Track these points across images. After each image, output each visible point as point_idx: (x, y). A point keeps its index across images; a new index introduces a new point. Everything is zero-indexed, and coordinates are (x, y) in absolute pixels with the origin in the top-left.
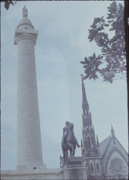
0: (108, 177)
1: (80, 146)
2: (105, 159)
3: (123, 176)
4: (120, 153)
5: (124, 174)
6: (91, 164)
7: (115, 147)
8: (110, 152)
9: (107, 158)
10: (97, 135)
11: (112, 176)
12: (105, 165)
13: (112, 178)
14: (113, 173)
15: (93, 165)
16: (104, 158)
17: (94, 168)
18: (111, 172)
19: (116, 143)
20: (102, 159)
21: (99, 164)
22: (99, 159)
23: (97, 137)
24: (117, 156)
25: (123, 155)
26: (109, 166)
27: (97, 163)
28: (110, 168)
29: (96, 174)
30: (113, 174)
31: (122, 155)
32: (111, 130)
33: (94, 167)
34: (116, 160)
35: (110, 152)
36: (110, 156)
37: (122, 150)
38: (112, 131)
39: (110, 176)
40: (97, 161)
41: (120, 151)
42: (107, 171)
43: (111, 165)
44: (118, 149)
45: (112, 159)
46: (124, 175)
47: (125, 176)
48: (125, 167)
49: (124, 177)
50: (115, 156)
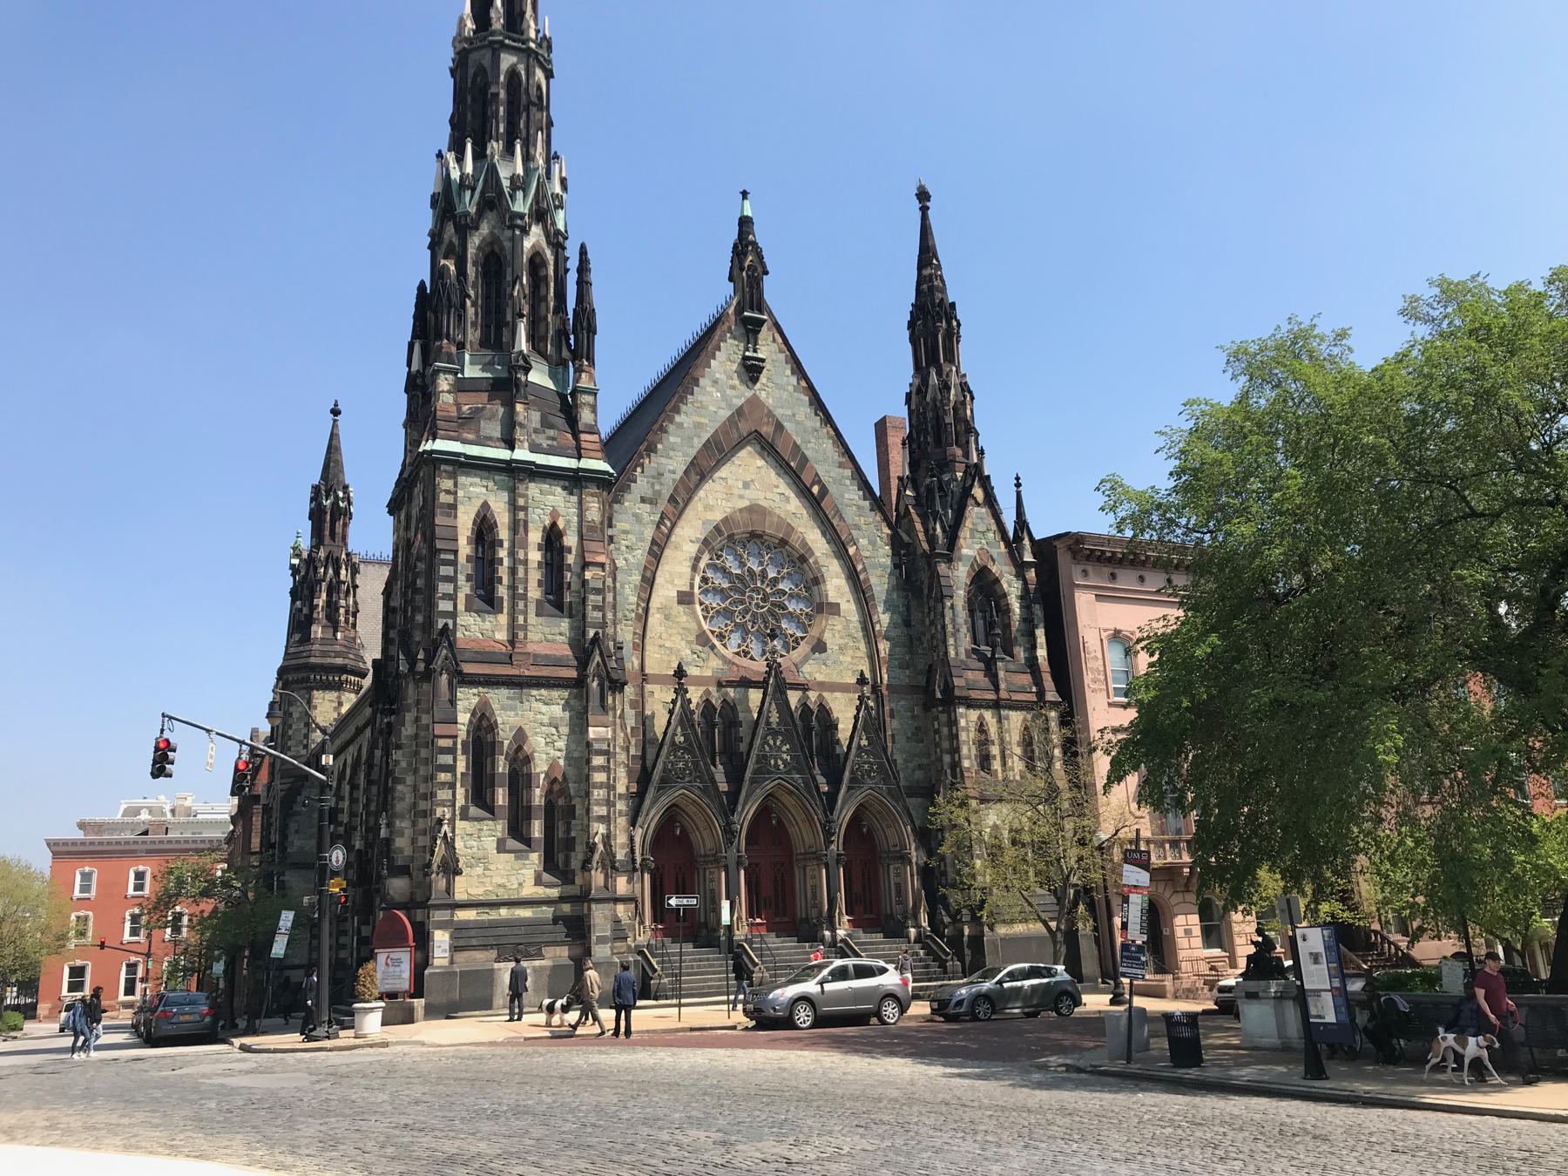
0: (660, 679)
2: (643, 500)
3: (803, 688)
4: (792, 468)
5: (813, 671)
6: (484, 529)
7: (754, 402)
10: (583, 251)
11: (699, 681)
12: (640, 555)
13: (695, 695)
14: (713, 647)
15: (504, 534)
16: (641, 485)
18: (692, 638)
19: (767, 365)
20: (612, 487)
21: (571, 540)
22: (575, 481)
23: (583, 268)
24: (757, 495)
25: (824, 491)
26: (676, 572)
27: (555, 514)
28: (685, 598)
29: (525, 628)
30: (715, 663)
31: (815, 489)
32: (735, 246)
33: (503, 553)
34: (745, 535)
35: (698, 444)
39: (680, 673)
42: (654, 619)
43: (694, 568)
44: (779, 427)
45: (718, 516)
46: (820, 678)
48: (835, 609)
49: (813, 695)
50: (746, 485)
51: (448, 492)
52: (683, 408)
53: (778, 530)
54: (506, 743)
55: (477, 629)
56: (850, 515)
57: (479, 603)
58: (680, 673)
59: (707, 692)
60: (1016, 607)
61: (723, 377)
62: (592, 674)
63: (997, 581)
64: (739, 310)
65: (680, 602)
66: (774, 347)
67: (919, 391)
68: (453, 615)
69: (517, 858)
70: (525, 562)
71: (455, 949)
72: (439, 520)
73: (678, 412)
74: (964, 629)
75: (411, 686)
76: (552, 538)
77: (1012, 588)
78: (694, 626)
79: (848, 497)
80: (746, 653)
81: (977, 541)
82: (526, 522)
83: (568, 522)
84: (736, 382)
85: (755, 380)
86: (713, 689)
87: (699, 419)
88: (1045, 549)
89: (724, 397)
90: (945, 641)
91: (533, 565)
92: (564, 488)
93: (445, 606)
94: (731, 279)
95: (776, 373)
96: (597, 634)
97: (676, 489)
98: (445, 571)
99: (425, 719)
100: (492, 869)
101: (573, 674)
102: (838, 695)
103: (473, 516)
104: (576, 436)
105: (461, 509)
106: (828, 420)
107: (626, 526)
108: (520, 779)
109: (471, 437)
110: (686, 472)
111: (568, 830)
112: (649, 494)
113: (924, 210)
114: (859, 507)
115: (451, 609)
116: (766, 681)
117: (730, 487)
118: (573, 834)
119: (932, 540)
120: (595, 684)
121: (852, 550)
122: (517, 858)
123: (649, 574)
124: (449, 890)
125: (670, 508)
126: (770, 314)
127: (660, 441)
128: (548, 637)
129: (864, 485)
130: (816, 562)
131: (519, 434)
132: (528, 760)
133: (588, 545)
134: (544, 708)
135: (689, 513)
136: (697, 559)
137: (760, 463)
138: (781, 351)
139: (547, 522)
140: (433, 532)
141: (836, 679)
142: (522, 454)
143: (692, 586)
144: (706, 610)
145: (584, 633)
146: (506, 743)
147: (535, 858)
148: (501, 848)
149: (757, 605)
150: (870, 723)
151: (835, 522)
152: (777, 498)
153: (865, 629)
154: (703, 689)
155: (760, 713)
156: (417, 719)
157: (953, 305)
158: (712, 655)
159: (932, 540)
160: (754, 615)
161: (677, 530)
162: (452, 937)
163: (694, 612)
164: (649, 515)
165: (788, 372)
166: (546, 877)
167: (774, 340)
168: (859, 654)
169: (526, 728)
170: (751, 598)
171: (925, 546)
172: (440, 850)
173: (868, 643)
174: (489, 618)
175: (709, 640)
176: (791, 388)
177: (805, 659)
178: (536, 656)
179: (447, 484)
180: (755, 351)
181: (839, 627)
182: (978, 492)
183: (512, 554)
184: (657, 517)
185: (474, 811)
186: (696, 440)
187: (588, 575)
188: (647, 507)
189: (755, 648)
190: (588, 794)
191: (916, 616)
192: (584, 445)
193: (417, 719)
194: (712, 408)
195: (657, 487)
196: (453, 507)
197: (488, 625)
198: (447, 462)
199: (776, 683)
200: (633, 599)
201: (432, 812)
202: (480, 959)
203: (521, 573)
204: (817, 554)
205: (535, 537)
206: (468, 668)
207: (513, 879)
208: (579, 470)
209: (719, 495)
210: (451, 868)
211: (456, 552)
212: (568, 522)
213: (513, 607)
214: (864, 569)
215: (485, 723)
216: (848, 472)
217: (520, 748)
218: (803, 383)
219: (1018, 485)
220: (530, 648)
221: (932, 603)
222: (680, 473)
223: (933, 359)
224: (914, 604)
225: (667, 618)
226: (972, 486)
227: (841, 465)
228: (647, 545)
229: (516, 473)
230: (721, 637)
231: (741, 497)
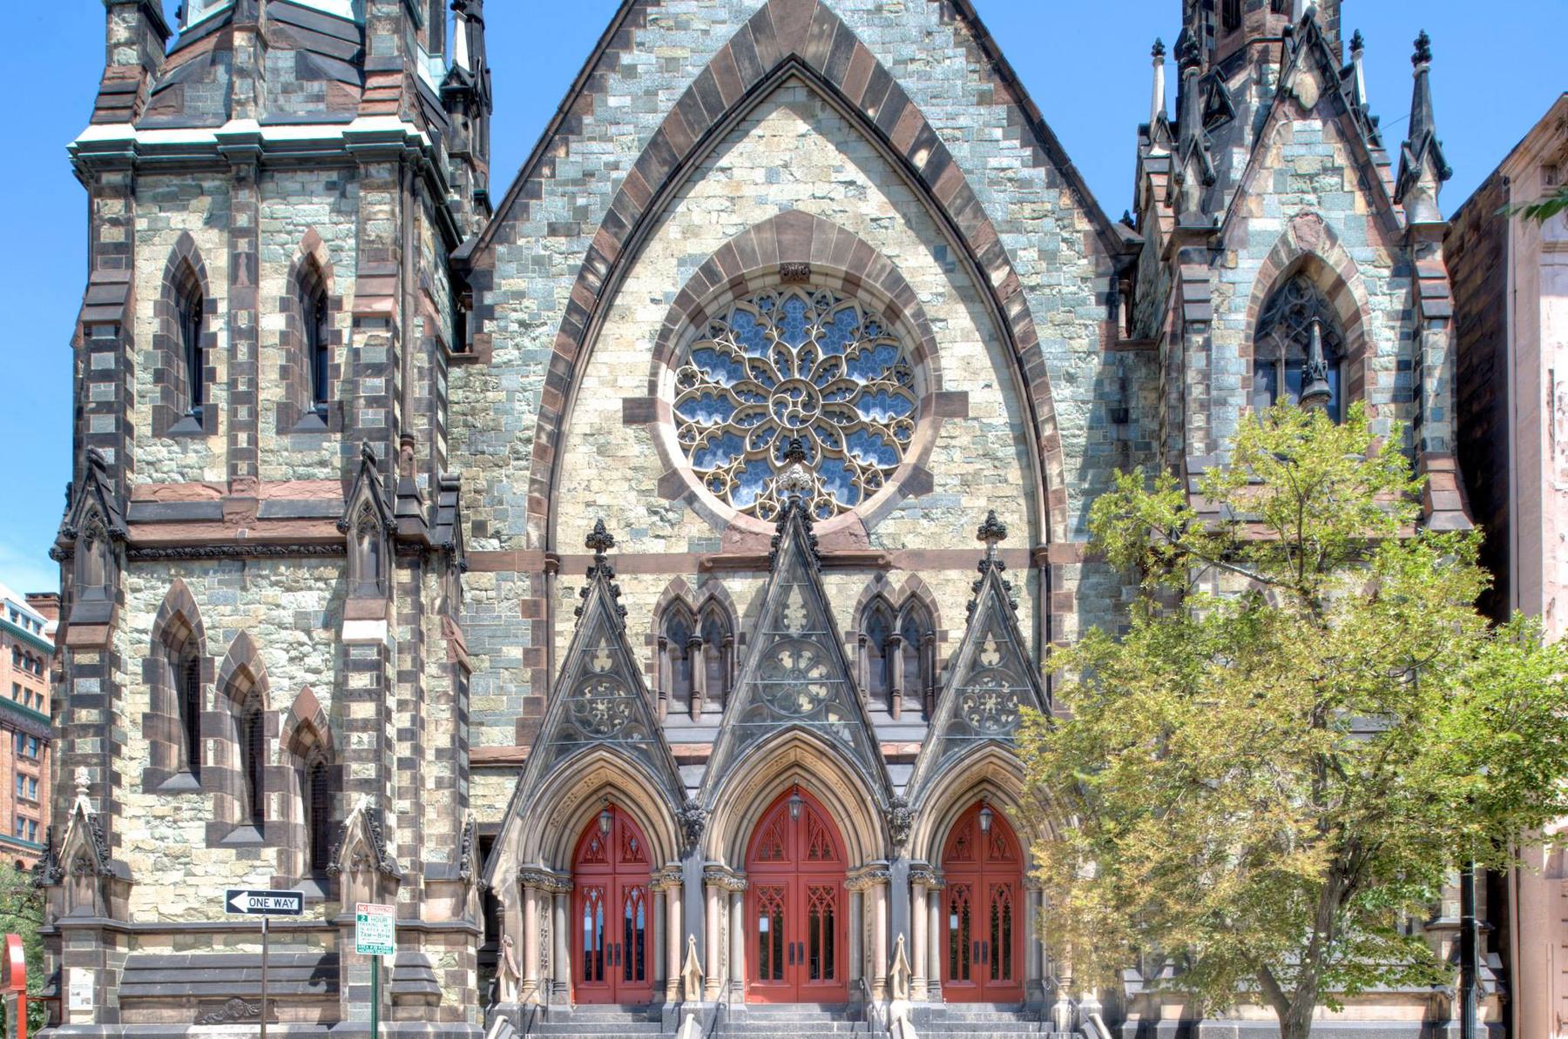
2: (553, 230)
5: (903, 531)
8: (686, 103)
14: (692, 499)
16: (549, 206)
25: (941, 159)
26: (624, 358)
28: (640, 412)
30: (696, 528)
31: (921, 159)
35: (666, 102)
41: (882, 75)
42: (577, 457)
44: (845, 38)
46: (913, 543)
47: (924, 575)
48: (955, 404)
56: (998, 204)
78: (655, 461)
87: (669, 53)
97: (619, 200)
102: (953, 574)
107: (519, 284)
110: (641, 163)
114: (1023, 183)
117: (739, 185)
121: (997, 277)
125: (607, 237)
127: (589, 109)
130: (919, 313)
135: (655, 248)
136: (664, 334)
137: (802, 126)
143: (653, 387)
144: (686, 434)
151: (962, 222)
152: (839, 193)
153: (1021, 439)
154: (665, 581)
158: (688, 511)
161: (630, 284)
164: (567, 254)
168: (1006, 490)
173: (1027, 467)
177: (885, 511)
181: (965, 440)
184: (579, 260)
186: (662, 95)
188: (561, 242)
195: (581, 201)
200: (531, 419)
204: (923, 296)
214: (1026, 313)
225: (602, 451)
227: (984, 99)
230: (715, 483)
231: (761, 201)
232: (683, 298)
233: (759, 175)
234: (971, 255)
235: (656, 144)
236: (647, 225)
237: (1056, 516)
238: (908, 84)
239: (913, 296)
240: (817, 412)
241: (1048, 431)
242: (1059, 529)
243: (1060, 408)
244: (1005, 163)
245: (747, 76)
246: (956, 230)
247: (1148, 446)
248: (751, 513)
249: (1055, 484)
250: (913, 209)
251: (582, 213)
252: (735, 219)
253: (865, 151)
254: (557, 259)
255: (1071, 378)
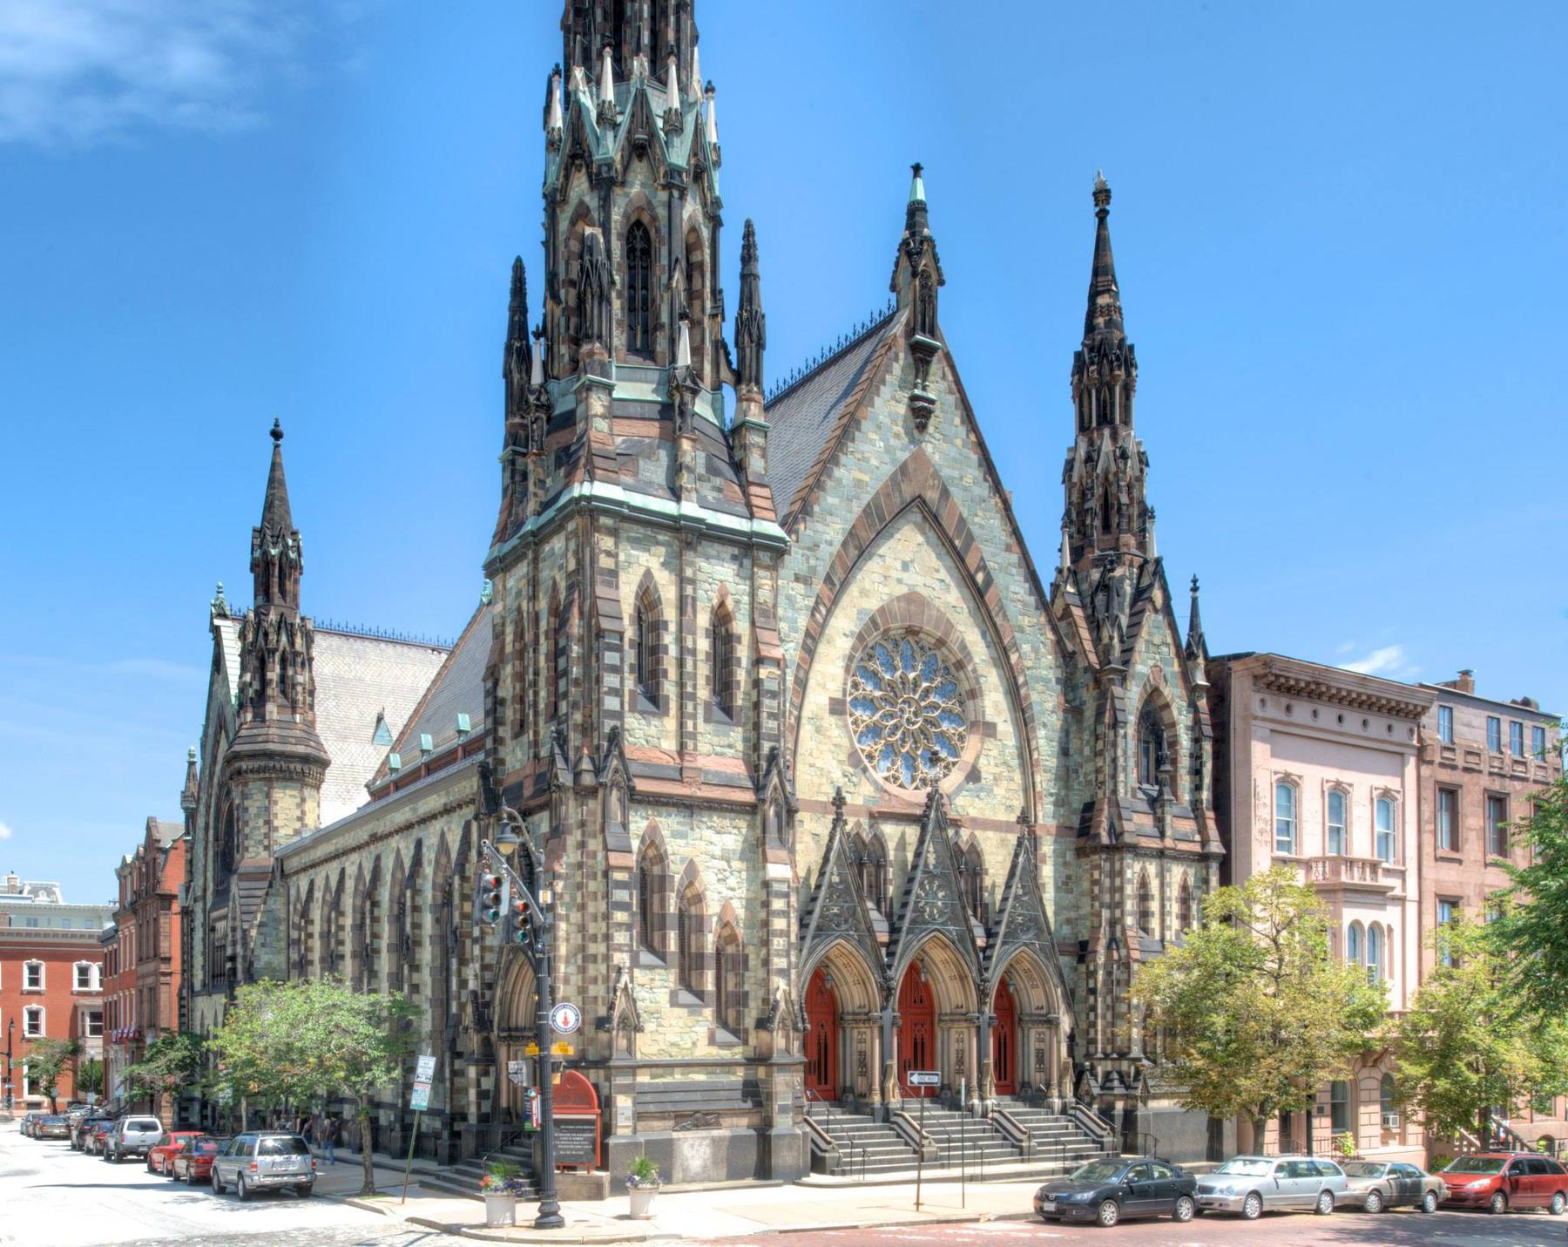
0: (816, 807)
1: (537, 335)
2: (797, 578)
3: (956, 824)
4: (955, 548)
5: (965, 805)
7: (919, 458)
8: (867, 511)
9: (822, 571)
11: (856, 811)
14: (865, 770)
15: (670, 614)
16: (795, 561)
17: (673, 651)
18: (843, 757)
19: (937, 408)
21: (741, 626)
22: (748, 549)
25: (989, 581)
28: (837, 707)
29: (694, 736)
30: (867, 789)
31: (980, 577)
33: (669, 639)
35: (857, 508)
36: (854, 553)
37: (986, 524)
38: (916, 256)
39: (839, 801)
40: (718, 575)
41: (962, 521)
43: (847, 669)
44: (945, 493)
45: (873, 605)
46: (973, 813)
47: (978, 833)
48: (989, 730)
50: (905, 567)
51: (609, 554)
52: (843, 459)
53: (937, 627)
54: (677, 877)
55: (649, 737)
56: (1013, 609)
57: (645, 704)
58: (839, 801)
59: (858, 824)
60: (1185, 741)
61: (887, 421)
62: (765, 800)
63: (1167, 706)
64: (910, 332)
65: (833, 712)
66: (943, 386)
67: (1089, 459)
68: (619, 715)
69: (691, 1014)
70: (694, 652)
71: (639, 1116)
72: (601, 591)
73: (837, 464)
74: (1132, 763)
75: (572, 803)
76: (721, 618)
77: (1181, 718)
78: (845, 742)
79: (1012, 589)
80: (896, 779)
81: (1152, 658)
82: (694, 599)
83: (737, 602)
84: (899, 429)
85: (922, 427)
86: (865, 821)
88: (1220, 670)
89: (889, 450)
90: (1114, 777)
91: (701, 656)
92: (734, 558)
93: (611, 703)
94: (893, 288)
95: (946, 418)
96: (773, 749)
97: (832, 567)
98: (610, 658)
99: (594, 844)
100: (673, 1029)
101: (749, 797)
102: (990, 834)
103: (634, 587)
104: (744, 486)
105: (623, 576)
106: (997, 487)
108: (690, 923)
109: (628, 480)
110: (844, 544)
111: (740, 984)
112: (802, 569)
113: (1102, 216)
114: (1025, 604)
115: (618, 708)
116: (926, 816)
117: (888, 568)
118: (746, 988)
119: (1105, 654)
120: (772, 812)
121: (1014, 658)
122: (691, 1014)
123: (802, 674)
124: (630, 1049)
125: (826, 590)
126: (942, 340)
128: (720, 753)
129: (1033, 578)
130: (974, 671)
131: (686, 480)
132: (699, 899)
133: (764, 635)
134: (715, 838)
135: (845, 600)
136: (851, 658)
137: (920, 539)
138: (951, 392)
139: (715, 602)
140: (594, 605)
141: (989, 814)
142: (689, 508)
144: (855, 723)
145: (756, 747)
146: (677, 877)
147: (709, 1012)
148: (674, 1002)
149: (908, 720)
150: (1024, 871)
151: (998, 620)
152: (937, 585)
153: (1021, 756)
155: (918, 855)
156: (582, 845)
157: (1131, 348)
159: (1105, 654)
160: (896, 727)
162: (635, 1103)
163: (846, 726)
165: (957, 421)
166: (723, 1035)
167: (944, 377)
168: (1014, 786)
169: (700, 862)
170: (902, 711)
171: (1093, 658)
172: (621, 1003)
173: (1024, 773)
174: (655, 722)
175: (860, 761)
176: (959, 442)
178: (707, 772)
179: (607, 542)
180: (924, 389)
181: (995, 753)
182: (1157, 595)
183: (680, 640)
184: (811, 602)
185: (646, 957)
187: (763, 672)
188: (800, 587)
189: (904, 776)
190: (766, 943)
191: (1074, 745)
192: (755, 501)
193: (582, 845)
194: (874, 462)
195: (812, 562)
196: (614, 573)
197: (653, 731)
198: (606, 512)
199: (932, 817)
201: (607, 958)
202: (658, 1130)
203: (689, 667)
204: (977, 660)
205: (703, 620)
206: (641, 785)
207: (686, 1037)
208: (753, 534)
209: (876, 578)
210: (632, 1025)
211: (621, 635)
212: (737, 602)
213: (681, 707)
215: (651, 853)
216: (1014, 558)
217: (691, 884)
218: (973, 437)
219: (1195, 589)
220: (701, 762)
221: (1101, 729)
222: (837, 546)
223: (1105, 419)
224: (1074, 728)
226: (1151, 586)
227: (1008, 549)
228: (800, 637)
229: (688, 537)
230: (870, 757)
231: (900, 581)
232: (860, 637)
233: (899, 565)
234: (1001, 642)
235: (852, 534)
236: (845, 584)
237: (1039, 808)
238: (975, 530)
239: (971, 659)
240: (920, 720)
241: (1035, 756)
242: (1040, 814)
243: (1042, 742)
244: (1017, 589)
245: (897, 503)
246: (994, 625)
247: (1076, 771)
248: (886, 779)
249: (1038, 789)
250: (972, 604)
251: (813, 570)
252: (886, 590)
253: (950, 563)
254: (799, 598)
255: (1045, 725)
